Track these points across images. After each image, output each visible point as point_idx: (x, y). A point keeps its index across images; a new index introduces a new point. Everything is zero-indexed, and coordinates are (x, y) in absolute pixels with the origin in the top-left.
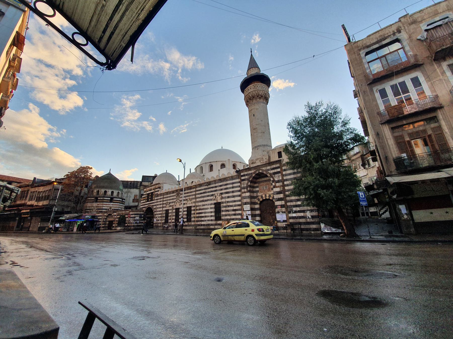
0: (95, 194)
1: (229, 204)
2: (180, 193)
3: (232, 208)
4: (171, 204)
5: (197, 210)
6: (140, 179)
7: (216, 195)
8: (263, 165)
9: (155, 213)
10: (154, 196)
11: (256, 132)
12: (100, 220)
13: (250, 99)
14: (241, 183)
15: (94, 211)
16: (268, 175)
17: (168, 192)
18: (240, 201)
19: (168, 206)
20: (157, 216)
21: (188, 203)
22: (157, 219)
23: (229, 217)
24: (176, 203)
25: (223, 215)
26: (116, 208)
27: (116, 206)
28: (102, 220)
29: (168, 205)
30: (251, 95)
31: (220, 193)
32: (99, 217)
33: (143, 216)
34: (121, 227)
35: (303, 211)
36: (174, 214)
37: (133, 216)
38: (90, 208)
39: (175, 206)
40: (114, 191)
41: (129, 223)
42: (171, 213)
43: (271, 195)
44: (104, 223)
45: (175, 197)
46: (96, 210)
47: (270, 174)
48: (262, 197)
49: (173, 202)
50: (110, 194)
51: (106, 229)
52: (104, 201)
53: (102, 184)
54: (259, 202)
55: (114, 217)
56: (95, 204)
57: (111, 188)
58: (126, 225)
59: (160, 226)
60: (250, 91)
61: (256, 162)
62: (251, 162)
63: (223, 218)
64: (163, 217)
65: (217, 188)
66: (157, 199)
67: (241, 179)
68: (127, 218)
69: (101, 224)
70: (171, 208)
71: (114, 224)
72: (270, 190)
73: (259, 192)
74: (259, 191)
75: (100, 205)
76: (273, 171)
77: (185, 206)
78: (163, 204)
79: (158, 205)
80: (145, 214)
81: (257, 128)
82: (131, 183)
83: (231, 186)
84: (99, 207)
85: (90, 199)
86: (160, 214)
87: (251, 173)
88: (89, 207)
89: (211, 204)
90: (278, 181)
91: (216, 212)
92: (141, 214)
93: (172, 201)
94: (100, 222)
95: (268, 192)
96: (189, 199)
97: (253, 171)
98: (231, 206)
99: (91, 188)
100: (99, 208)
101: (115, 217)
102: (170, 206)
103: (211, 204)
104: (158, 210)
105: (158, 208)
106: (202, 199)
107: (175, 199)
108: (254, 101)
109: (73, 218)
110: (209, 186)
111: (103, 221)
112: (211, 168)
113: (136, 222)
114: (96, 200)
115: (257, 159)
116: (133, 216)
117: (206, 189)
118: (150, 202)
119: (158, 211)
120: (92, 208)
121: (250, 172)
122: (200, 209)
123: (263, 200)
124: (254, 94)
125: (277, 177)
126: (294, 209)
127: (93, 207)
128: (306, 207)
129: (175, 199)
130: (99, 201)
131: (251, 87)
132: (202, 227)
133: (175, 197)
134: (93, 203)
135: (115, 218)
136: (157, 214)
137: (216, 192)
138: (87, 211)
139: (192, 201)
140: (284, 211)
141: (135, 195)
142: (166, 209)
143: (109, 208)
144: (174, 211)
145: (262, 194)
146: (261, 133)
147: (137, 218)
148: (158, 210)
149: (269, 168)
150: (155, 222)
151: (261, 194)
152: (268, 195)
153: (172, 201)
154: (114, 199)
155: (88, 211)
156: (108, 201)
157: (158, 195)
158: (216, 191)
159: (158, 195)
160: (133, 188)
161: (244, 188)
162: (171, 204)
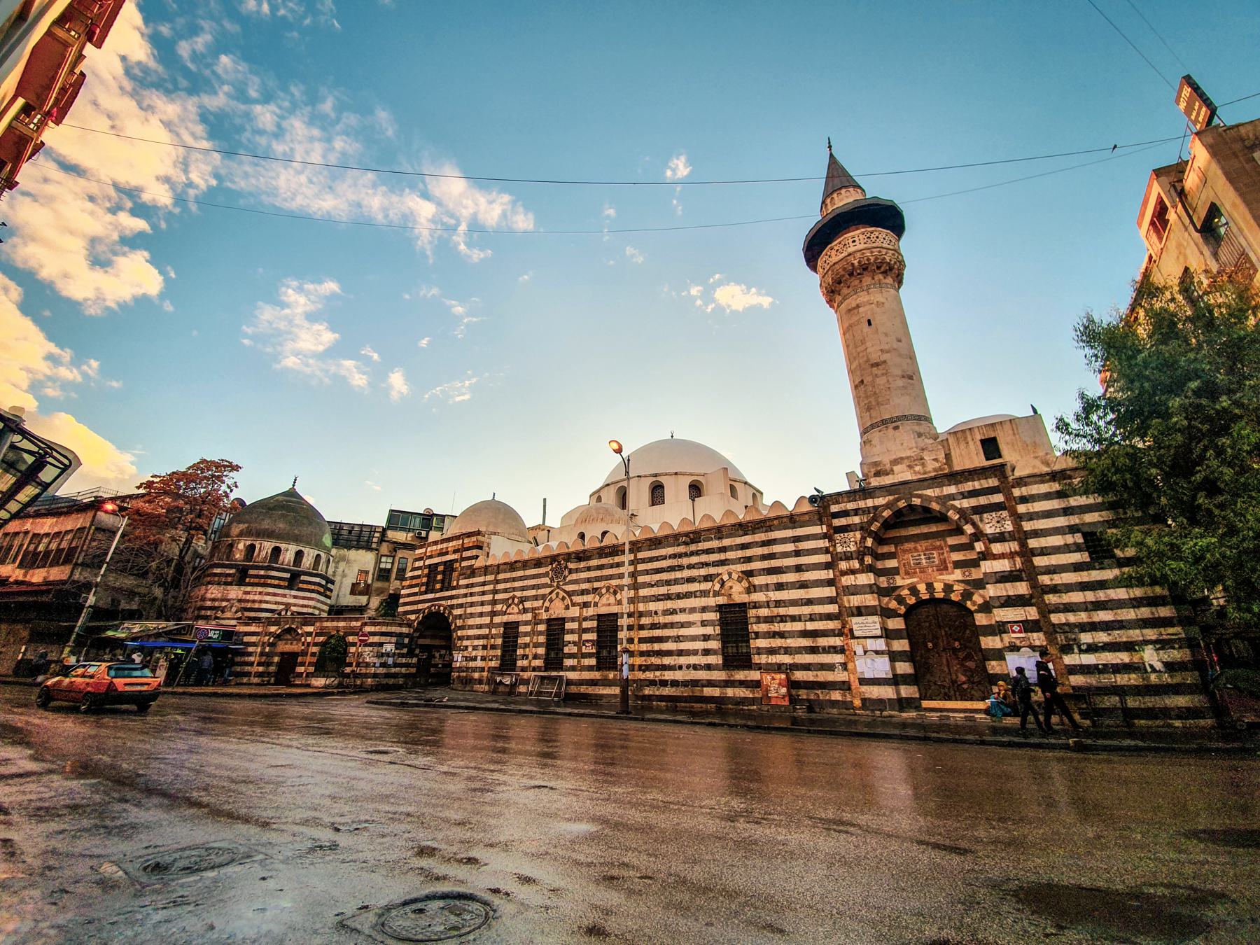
0: (237, 556)
1: (782, 611)
2: (566, 567)
3: (798, 626)
4: (528, 605)
5: (641, 627)
6: (382, 522)
7: (726, 577)
8: (925, 480)
9: (459, 633)
10: (455, 574)
11: (883, 375)
12: (251, 649)
13: (851, 274)
14: (831, 539)
15: (228, 615)
16: (951, 513)
17: (516, 562)
18: (831, 600)
19: (516, 610)
20: (466, 643)
21: (604, 600)
22: (466, 654)
23: (787, 659)
24: (551, 600)
25: (759, 651)
26: (305, 610)
27: (306, 602)
28: (259, 650)
29: (517, 605)
30: (856, 262)
31: (742, 572)
32: (246, 639)
33: (406, 641)
34: (327, 677)
35: (1129, 647)
36: (542, 639)
37: (376, 639)
38: (217, 604)
39: (547, 610)
40: (306, 550)
41: (358, 665)
42: (526, 634)
43: (955, 588)
44: (264, 659)
45: (547, 580)
46: (236, 612)
47: (961, 512)
48: (913, 590)
49: (536, 598)
50: (290, 561)
51: (269, 683)
52: (269, 581)
53: (266, 524)
54: (902, 610)
55: (303, 639)
56: (235, 592)
57: (296, 539)
58: (348, 670)
59: (480, 682)
60: (851, 250)
61: (892, 470)
62: (873, 470)
63: (756, 659)
64: (493, 647)
65: (731, 555)
66: (467, 586)
67: (830, 526)
68: (354, 644)
69: (251, 664)
70: (529, 617)
71: (302, 664)
72: (946, 568)
73: (898, 574)
74: (902, 571)
75: (254, 594)
76: (973, 502)
77: (590, 612)
78: (494, 602)
79: (472, 604)
80: (416, 634)
81: (885, 362)
82: (350, 532)
83: (790, 547)
84: (248, 601)
85: (218, 571)
86: (479, 637)
87: (876, 508)
88: (213, 600)
89: (704, 610)
90: (1001, 538)
91: (725, 637)
92: (400, 635)
93: (533, 592)
94: (250, 654)
96: (608, 588)
97: (881, 501)
98: (794, 619)
99: (228, 535)
100: (249, 605)
101: (309, 639)
102: (525, 611)
103: (704, 610)
104: (471, 622)
105: (472, 615)
106: (663, 590)
107: (545, 586)
108: (867, 280)
109: (158, 635)
110: (693, 547)
111: (262, 654)
112: (657, 493)
113: (383, 660)
114: (242, 576)
115: (896, 462)
116: (376, 639)
117: (680, 556)
118: (438, 595)
119: (471, 627)
120: (224, 604)
121: (870, 503)
122: (654, 626)
123: (921, 603)
124: (868, 260)
125: (994, 522)
126: (1086, 638)
127: (228, 600)
128: (1137, 631)
129: (545, 586)
130: (252, 580)
131: (856, 239)
132: (667, 691)
133: (547, 580)
134: (229, 587)
135: (309, 644)
136: (469, 638)
137: (726, 568)
138: (203, 613)
139: (618, 596)
140: (1037, 643)
141: (361, 572)
142: (505, 619)
143: (283, 607)
144: (542, 627)
146: (903, 377)
147: (389, 648)
148: (471, 622)
149: (952, 489)
150: (458, 665)
151: (909, 581)
152: (939, 587)
153: (533, 592)
154: (303, 578)
155: (209, 613)
156: (282, 583)
157: (473, 572)
158: (723, 563)
159: (473, 572)
160: (358, 547)
161: (848, 557)
162: (528, 605)
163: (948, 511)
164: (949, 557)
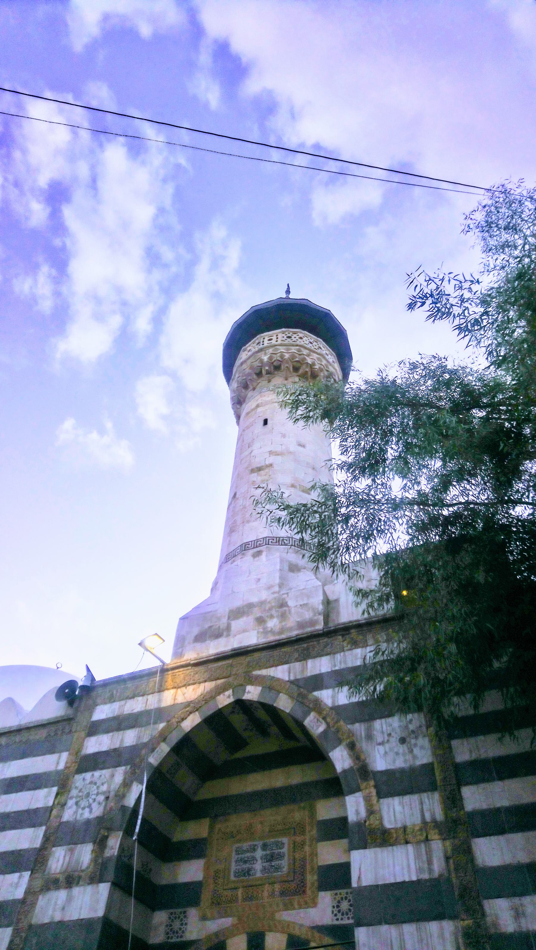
72: (301, 890)
74: (206, 896)
81: (271, 465)
95: (288, 907)
124: (282, 356)
145: (226, 922)
163: (306, 714)
164: (314, 854)
